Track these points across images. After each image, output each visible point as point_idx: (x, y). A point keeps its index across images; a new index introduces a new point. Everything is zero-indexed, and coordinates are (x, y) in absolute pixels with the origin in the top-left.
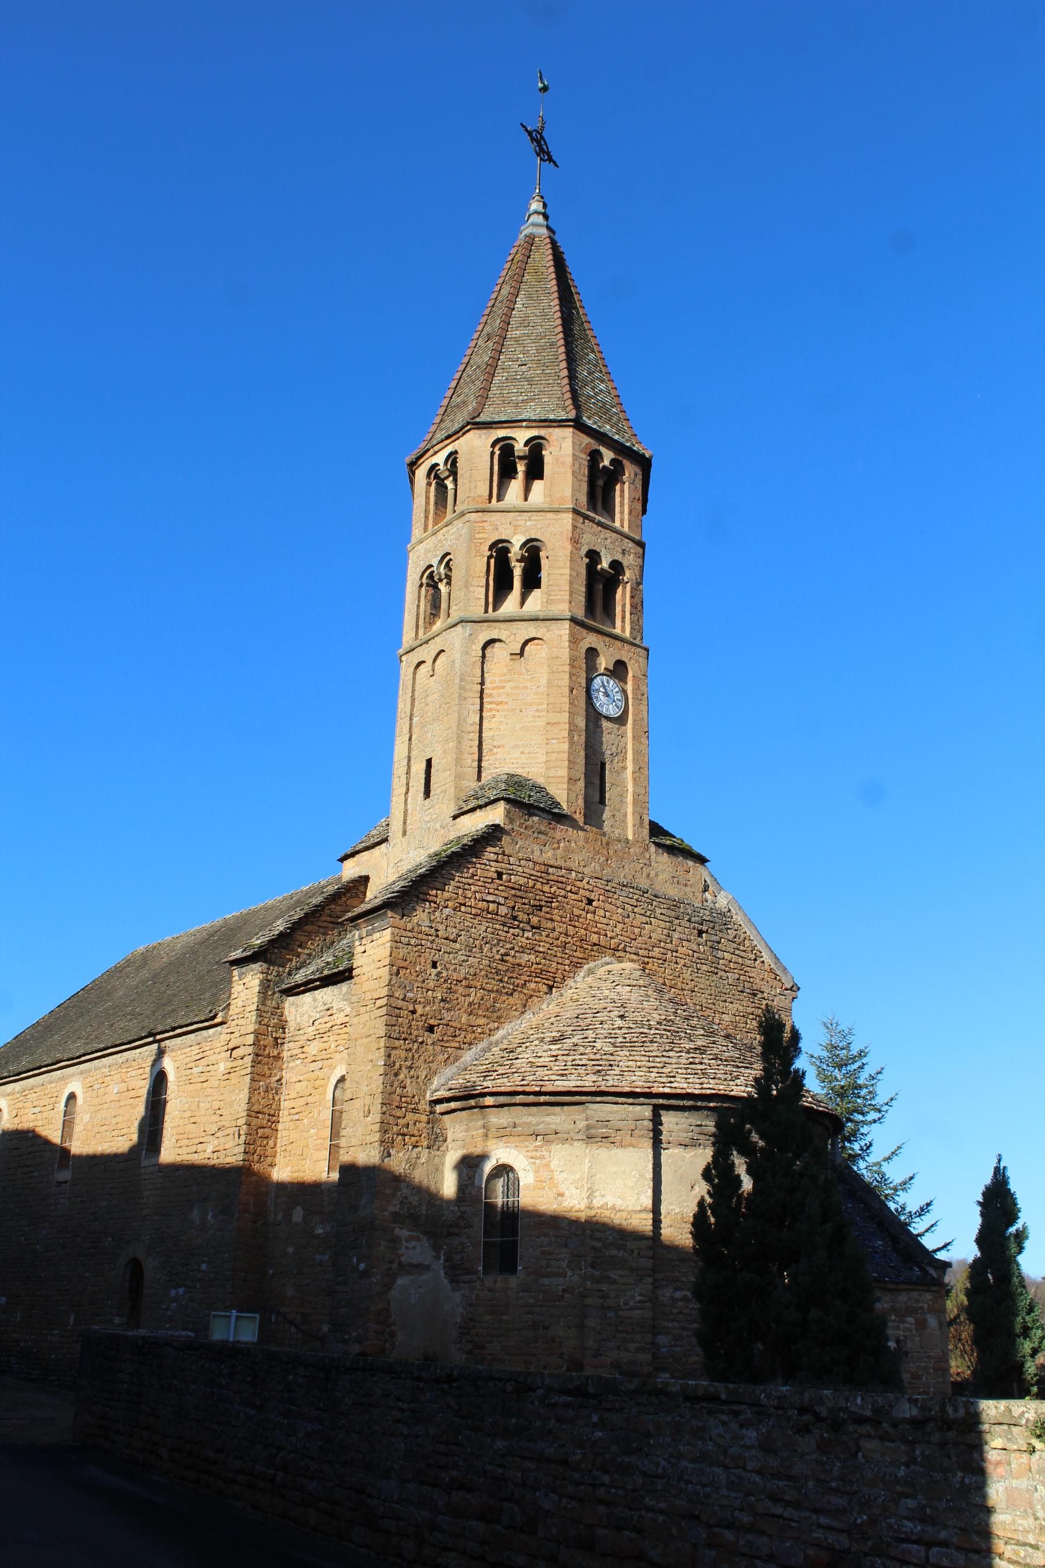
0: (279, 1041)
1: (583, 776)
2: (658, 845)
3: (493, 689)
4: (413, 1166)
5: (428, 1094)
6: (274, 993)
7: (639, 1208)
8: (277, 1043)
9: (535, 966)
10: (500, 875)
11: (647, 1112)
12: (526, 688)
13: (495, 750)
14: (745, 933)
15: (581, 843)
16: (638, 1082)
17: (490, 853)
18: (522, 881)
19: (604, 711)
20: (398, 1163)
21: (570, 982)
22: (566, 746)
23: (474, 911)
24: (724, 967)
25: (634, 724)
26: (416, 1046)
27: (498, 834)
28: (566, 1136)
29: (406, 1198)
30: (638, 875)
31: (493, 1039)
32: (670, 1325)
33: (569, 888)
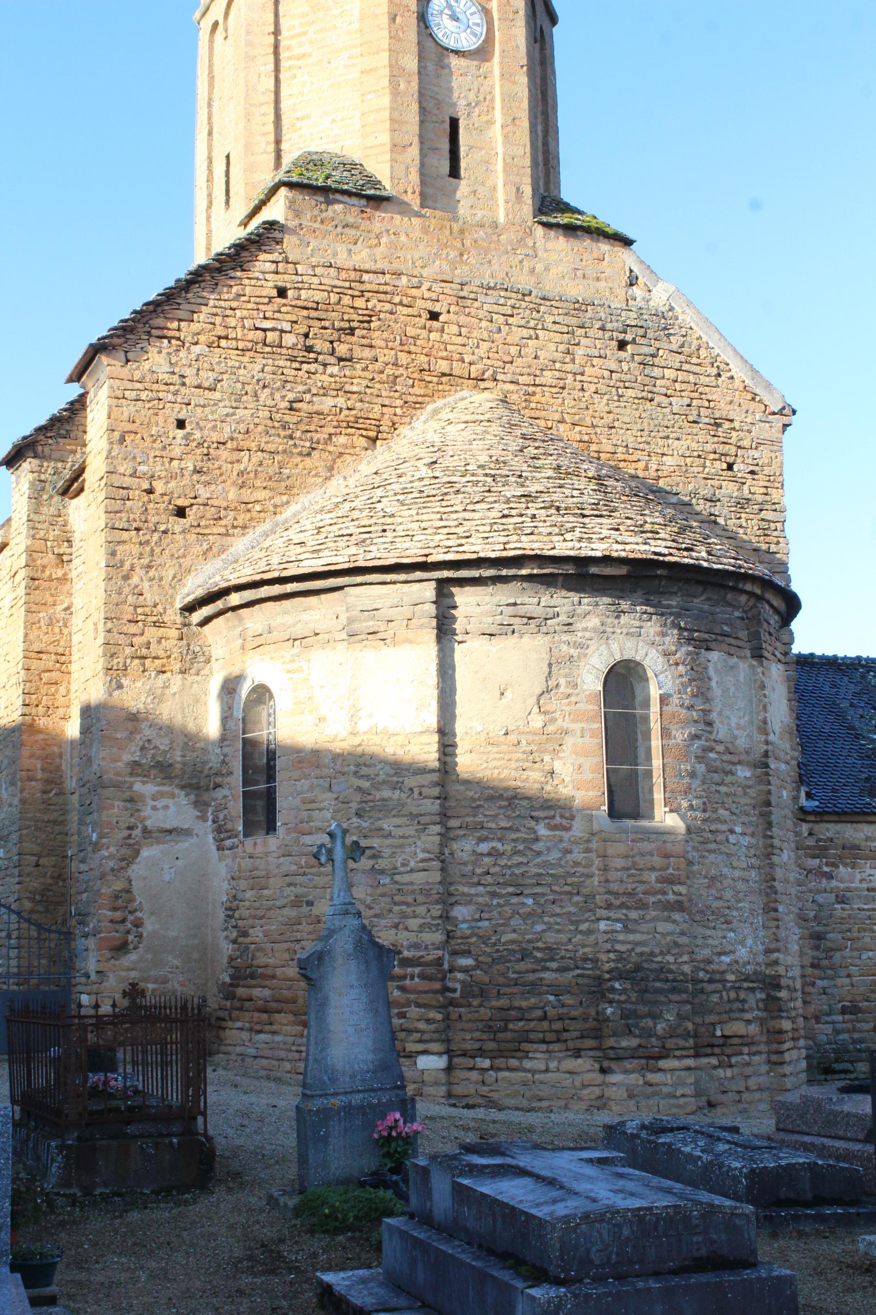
0: (65, 558)
1: (416, 140)
2: (547, 225)
3: (292, 37)
4: (160, 699)
5: (178, 598)
6: (51, 497)
7: (419, 730)
8: (61, 560)
9: (345, 412)
10: (282, 292)
11: (428, 591)
12: (335, 27)
13: (299, 124)
14: (699, 338)
15: (418, 234)
16: (411, 552)
17: (263, 262)
18: (319, 296)
19: (452, 44)
20: (135, 695)
21: (403, 430)
22: (386, 100)
23: (241, 345)
24: (664, 391)
25: (502, 57)
26: (156, 536)
27: (277, 235)
28: (327, 636)
29: (149, 741)
30: (515, 271)
31: (279, 518)
32: (473, 891)
33: (397, 299)
